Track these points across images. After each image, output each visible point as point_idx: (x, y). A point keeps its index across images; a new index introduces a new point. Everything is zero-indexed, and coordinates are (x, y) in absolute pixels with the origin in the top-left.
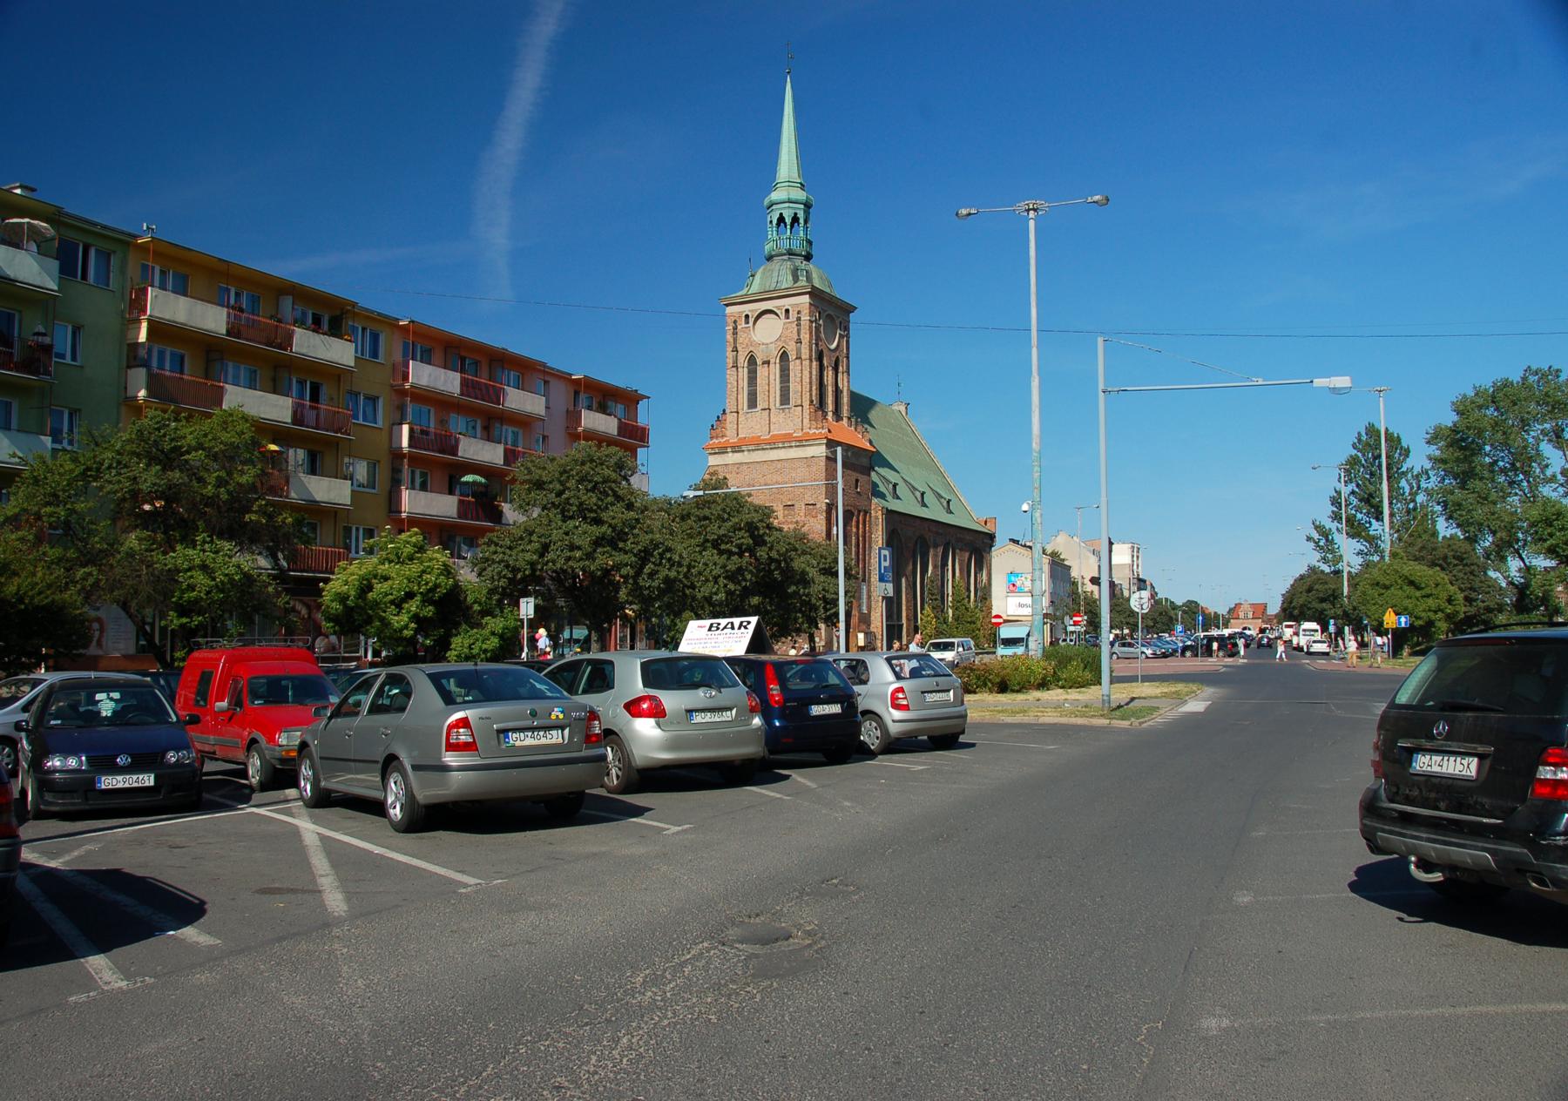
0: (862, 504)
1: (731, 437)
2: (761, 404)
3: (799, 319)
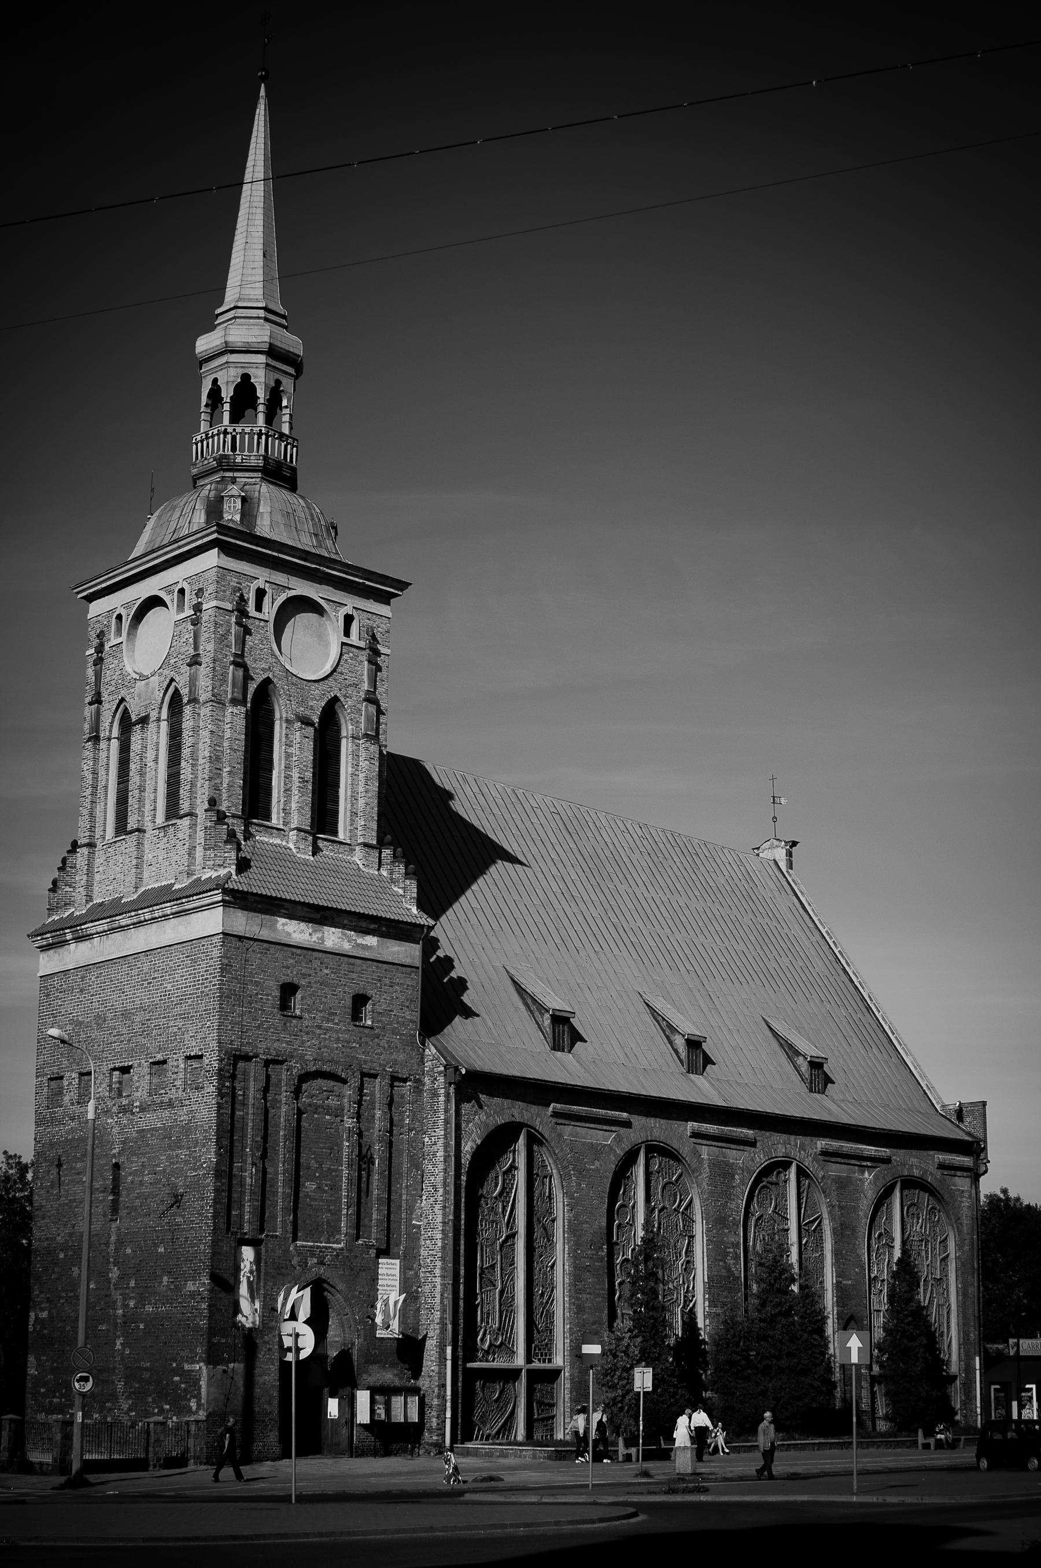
1: (79, 910)
2: (132, 823)
3: (198, 608)
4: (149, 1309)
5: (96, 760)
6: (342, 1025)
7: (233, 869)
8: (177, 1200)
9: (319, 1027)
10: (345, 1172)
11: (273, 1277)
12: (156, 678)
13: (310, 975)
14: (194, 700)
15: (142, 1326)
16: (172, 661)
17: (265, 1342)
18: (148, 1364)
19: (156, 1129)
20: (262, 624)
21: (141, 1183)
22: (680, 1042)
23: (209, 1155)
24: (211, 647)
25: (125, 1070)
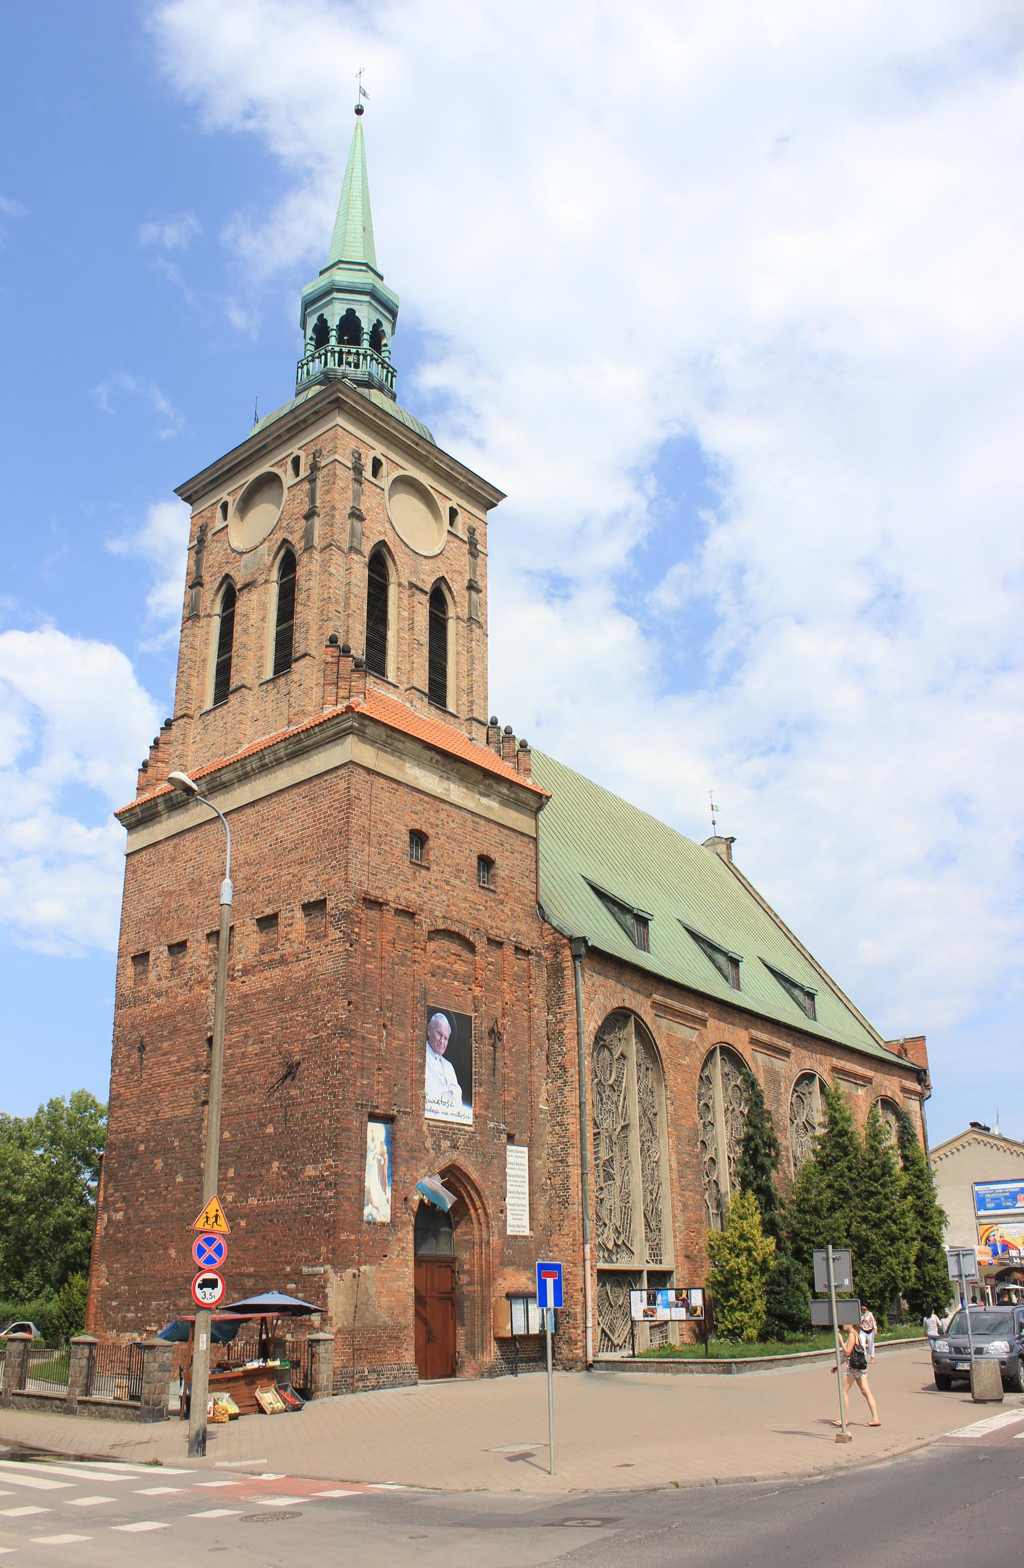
8: (291, 1071)
9: (448, 883)
11: (406, 1161)
12: (266, 544)
13: (437, 826)
15: (243, 1223)
16: (284, 524)
17: (400, 1240)
18: (252, 1269)
19: (264, 992)
20: (378, 490)
21: (244, 1055)
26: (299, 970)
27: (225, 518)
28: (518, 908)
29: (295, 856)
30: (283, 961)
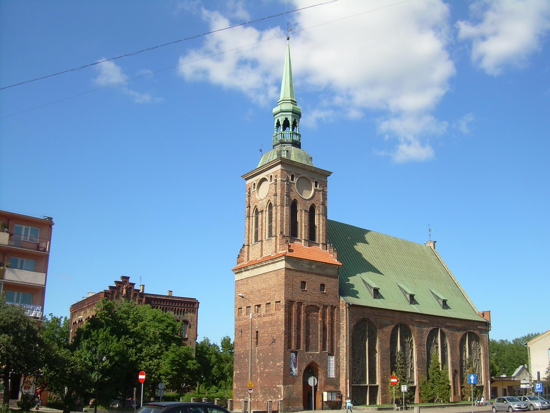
0: (329, 301)
1: (245, 263)
2: (259, 239)
3: (276, 180)
4: (267, 370)
5: (249, 222)
6: (318, 292)
7: (287, 250)
8: (274, 341)
10: (319, 333)
14: (276, 205)
22: (408, 296)
23: (283, 328)
24: (280, 190)
25: (259, 306)
26: (275, 317)
27: (254, 188)
28: (332, 296)
29: (273, 289)
30: (272, 315)
